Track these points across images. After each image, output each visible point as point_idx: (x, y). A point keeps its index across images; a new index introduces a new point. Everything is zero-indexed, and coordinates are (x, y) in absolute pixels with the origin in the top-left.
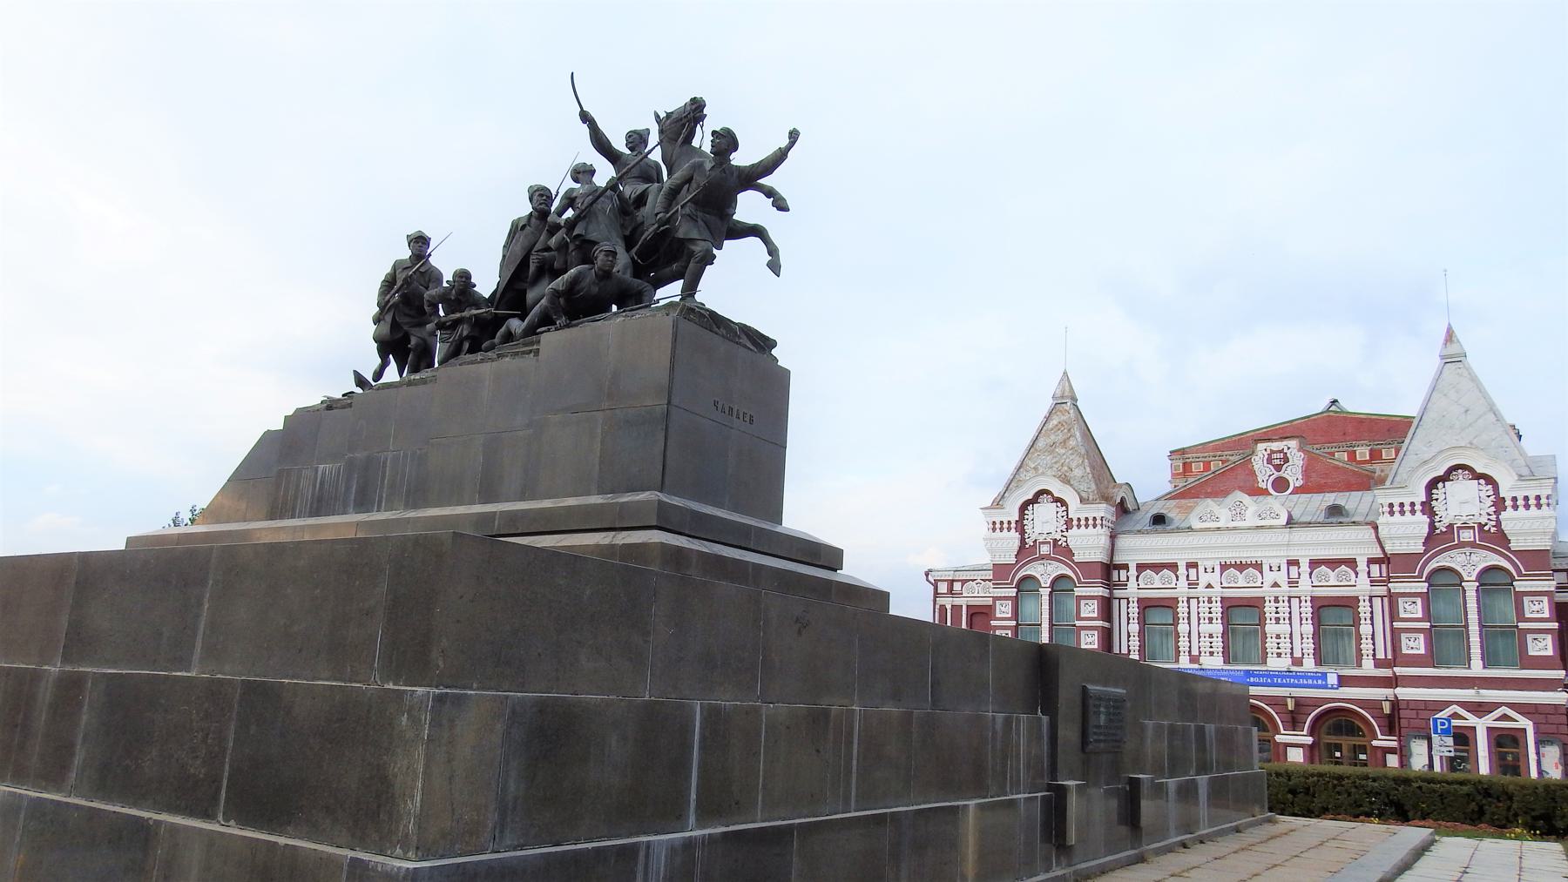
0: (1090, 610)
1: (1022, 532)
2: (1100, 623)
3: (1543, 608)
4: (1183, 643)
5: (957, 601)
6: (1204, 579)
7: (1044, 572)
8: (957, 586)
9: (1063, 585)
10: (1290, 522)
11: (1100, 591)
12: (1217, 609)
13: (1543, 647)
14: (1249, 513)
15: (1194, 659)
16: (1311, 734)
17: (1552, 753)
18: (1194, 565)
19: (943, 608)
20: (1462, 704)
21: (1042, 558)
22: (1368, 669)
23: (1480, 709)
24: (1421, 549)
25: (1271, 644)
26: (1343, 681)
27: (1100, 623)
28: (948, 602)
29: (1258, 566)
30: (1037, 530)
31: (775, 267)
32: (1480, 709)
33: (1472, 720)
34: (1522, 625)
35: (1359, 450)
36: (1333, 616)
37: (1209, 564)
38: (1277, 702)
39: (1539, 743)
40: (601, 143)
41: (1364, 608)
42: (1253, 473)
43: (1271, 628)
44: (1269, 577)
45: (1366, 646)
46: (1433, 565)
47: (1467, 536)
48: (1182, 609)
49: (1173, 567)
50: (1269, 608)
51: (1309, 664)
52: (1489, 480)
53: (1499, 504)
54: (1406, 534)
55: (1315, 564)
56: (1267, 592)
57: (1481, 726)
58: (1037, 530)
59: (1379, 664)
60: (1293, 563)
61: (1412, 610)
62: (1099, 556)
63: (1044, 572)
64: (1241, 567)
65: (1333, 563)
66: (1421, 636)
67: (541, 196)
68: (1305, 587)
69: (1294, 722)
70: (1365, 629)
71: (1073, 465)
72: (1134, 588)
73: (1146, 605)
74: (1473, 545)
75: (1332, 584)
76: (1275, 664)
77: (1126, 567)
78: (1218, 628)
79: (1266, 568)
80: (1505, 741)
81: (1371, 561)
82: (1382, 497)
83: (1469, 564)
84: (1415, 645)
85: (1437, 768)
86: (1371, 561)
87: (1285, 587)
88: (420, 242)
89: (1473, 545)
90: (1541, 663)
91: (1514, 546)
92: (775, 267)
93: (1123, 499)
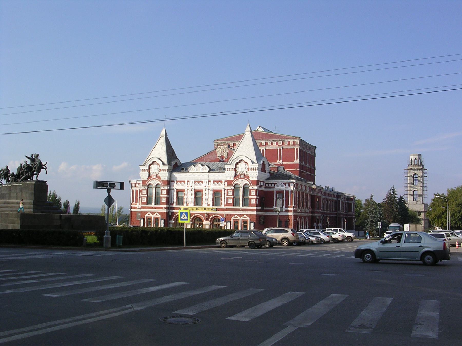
0: (164, 192)
1: (149, 172)
2: (166, 196)
3: (253, 193)
4: (185, 201)
5: (138, 189)
6: (191, 185)
7: (154, 183)
8: (137, 185)
9: (158, 186)
10: (209, 172)
11: (166, 188)
12: (193, 192)
13: (253, 202)
14: (201, 169)
15: (187, 205)
16: (210, 222)
17: (252, 224)
18: (189, 181)
19: (133, 191)
20: (238, 215)
21: (154, 179)
22: (223, 207)
23: (241, 216)
24: (233, 179)
25: (203, 201)
26: (217, 210)
27: (166, 196)
28: (134, 189)
29: (202, 182)
30: (153, 172)
31: (46, 173)
32: (241, 216)
33: (239, 218)
34: (250, 197)
35: (262, 142)
36: (216, 193)
37: (192, 181)
38: (203, 215)
39: (250, 223)
40: (28, 157)
41: (223, 193)
42: (216, 154)
43: (204, 197)
44: (204, 184)
45: (223, 201)
46: (234, 184)
47: (242, 176)
48: (185, 192)
49: (184, 182)
50: (204, 192)
51: (211, 205)
52: (247, 164)
53: (248, 169)
54: (229, 175)
55: (214, 182)
56: (203, 188)
57: (240, 219)
58: (153, 172)
59: (224, 206)
60: (209, 181)
61: (231, 193)
62: (166, 179)
63: (154, 183)
64: (199, 182)
65: (218, 182)
66: (231, 199)
67: (21, 164)
68: (211, 188)
69: (207, 220)
70: (223, 197)
71: (163, 154)
72: (176, 186)
73: (178, 191)
74: (243, 178)
75: (217, 187)
76: (205, 206)
77: (174, 181)
78: (193, 197)
79: (204, 182)
80: (245, 222)
81: (225, 181)
82: (227, 167)
83: (241, 182)
84: (230, 201)
85: (232, 229)
86: (225, 181)
87: (207, 187)
88: (7, 167)
89: (243, 178)
90: (252, 205)
91: (250, 179)
92: (46, 173)
93: (176, 163)
